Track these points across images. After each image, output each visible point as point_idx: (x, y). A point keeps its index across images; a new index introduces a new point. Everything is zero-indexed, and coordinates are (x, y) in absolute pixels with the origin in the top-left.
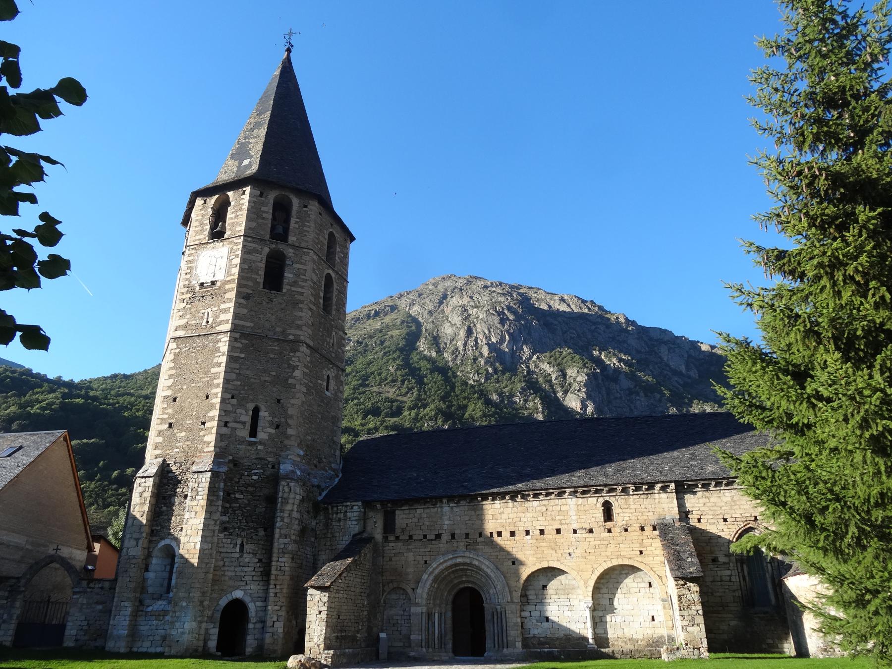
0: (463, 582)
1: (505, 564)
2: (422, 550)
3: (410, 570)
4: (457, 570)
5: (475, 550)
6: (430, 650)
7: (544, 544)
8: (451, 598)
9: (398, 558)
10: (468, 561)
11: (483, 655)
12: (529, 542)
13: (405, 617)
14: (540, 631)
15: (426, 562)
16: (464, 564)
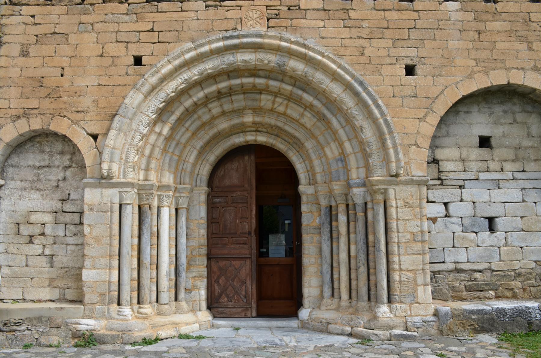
0: (242, 129)
1: (387, 70)
2: (123, 27)
3: (87, 81)
4: (231, 92)
5: (295, 29)
6: (147, 309)
7: (497, 25)
8: (205, 170)
9: (47, 50)
10: (271, 59)
11: (294, 315)
12: (455, 16)
13: (68, 218)
14: (474, 253)
15: (138, 61)
16: (254, 72)
